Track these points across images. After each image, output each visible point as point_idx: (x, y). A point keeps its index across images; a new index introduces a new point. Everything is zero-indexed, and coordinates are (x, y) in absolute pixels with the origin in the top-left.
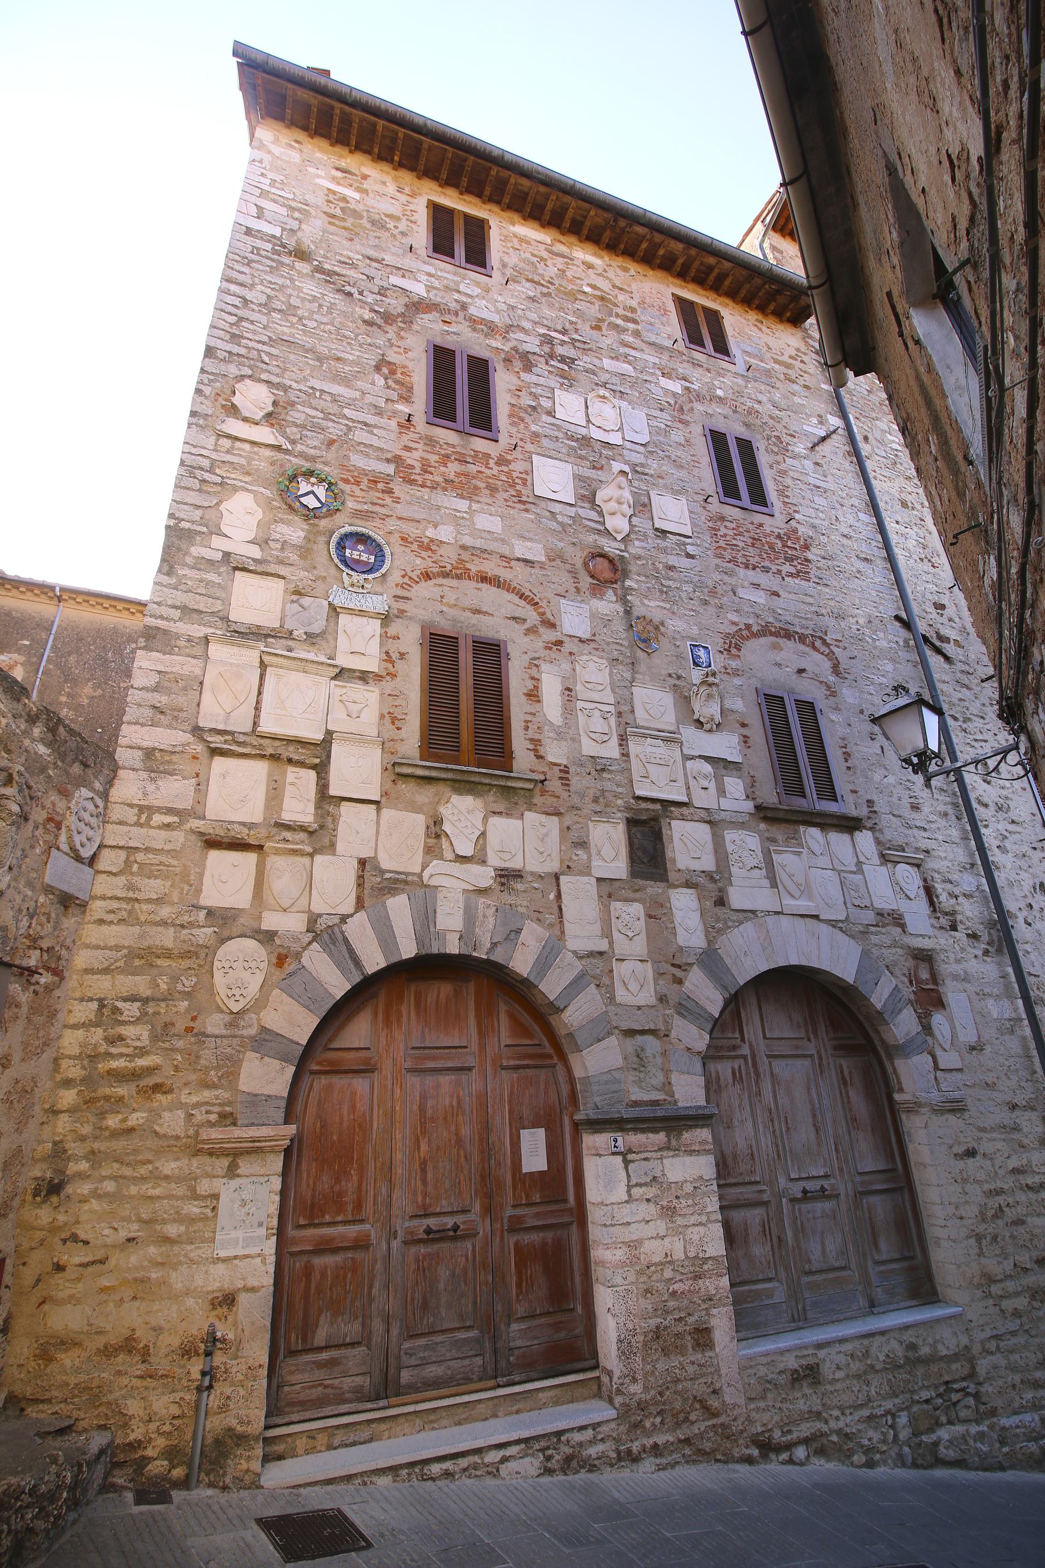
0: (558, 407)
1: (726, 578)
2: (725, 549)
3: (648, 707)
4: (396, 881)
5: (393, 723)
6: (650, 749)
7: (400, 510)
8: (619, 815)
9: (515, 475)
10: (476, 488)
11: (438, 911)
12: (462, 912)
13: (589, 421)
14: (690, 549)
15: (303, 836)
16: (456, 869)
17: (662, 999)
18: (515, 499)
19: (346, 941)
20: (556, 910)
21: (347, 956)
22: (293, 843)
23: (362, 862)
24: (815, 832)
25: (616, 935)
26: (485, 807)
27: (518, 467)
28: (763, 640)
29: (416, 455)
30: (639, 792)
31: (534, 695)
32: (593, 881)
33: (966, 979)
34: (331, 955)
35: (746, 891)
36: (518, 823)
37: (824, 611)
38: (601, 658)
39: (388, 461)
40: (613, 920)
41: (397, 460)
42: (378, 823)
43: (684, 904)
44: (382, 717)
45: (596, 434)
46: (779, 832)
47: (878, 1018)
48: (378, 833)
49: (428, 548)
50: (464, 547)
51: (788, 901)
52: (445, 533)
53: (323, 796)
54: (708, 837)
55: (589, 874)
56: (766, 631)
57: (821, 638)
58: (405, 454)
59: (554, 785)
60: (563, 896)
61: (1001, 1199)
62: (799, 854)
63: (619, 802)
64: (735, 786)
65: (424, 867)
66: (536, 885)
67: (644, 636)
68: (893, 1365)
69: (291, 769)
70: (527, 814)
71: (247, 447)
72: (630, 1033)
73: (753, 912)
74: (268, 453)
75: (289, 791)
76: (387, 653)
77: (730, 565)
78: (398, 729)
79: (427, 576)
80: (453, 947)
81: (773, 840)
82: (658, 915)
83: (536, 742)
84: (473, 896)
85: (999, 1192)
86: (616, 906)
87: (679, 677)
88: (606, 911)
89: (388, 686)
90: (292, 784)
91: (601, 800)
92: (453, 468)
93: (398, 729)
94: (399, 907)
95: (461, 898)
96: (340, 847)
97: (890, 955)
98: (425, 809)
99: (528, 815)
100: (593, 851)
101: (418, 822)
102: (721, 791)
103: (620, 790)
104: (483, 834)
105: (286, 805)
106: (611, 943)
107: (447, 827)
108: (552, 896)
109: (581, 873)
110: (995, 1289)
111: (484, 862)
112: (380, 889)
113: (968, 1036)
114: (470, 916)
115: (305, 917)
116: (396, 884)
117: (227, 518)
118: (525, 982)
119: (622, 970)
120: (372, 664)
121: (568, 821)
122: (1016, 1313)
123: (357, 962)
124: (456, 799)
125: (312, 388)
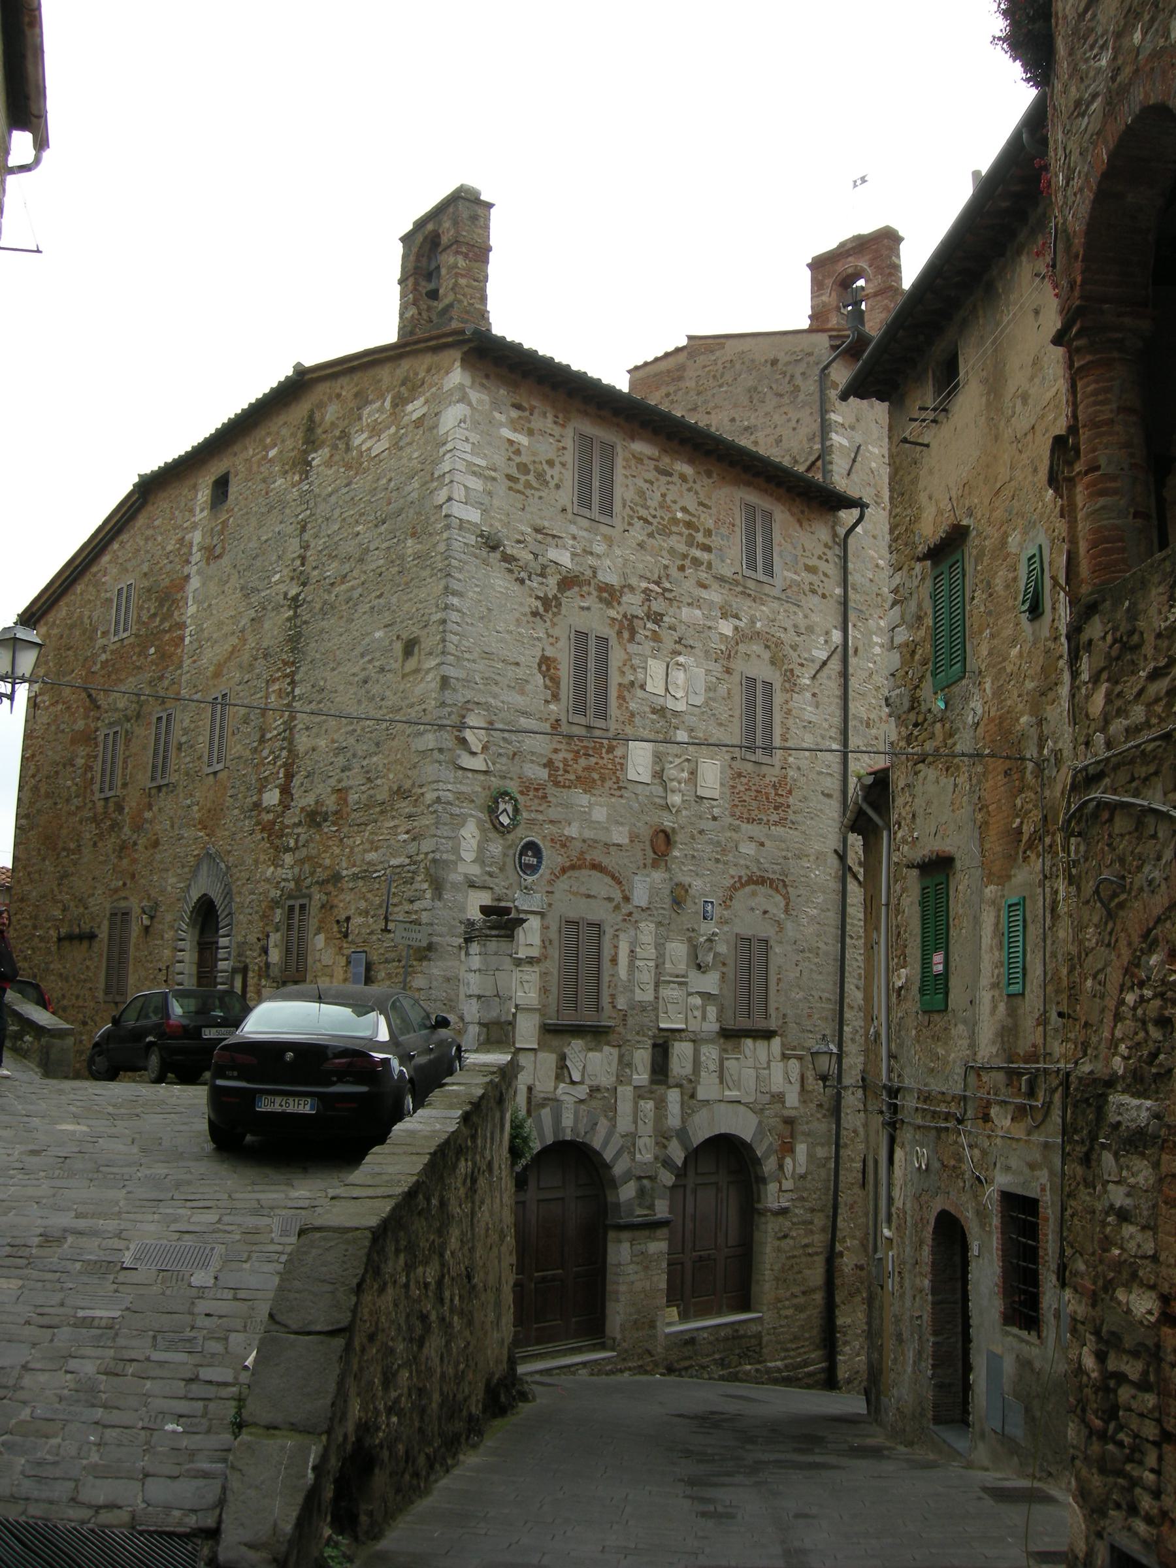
0: (649, 680)
1: (733, 834)
2: (737, 806)
4: (545, 1099)
7: (553, 813)
9: (617, 760)
10: (594, 781)
13: (667, 690)
14: (716, 811)
17: (656, 1158)
18: (615, 786)
24: (749, 1042)
25: (640, 1122)
27: (618, 752)
28: (748, 889)
29: (561, 756)
30: (662, 1026)
31: (614, 961)
32: (630, 1088)
33: (808, 1134)
35: (707, 1089)
37: (790, 855)
38: (652, 922)
39: (545, 766)
41: (549, 764)
43: (674, 1096)
45: (671, 704)
46: (729, 1045)
47: (757, 1162)
49: (564, 846)
50: (584, 841)
51: (727, 1093)
52: (572, 831)
54: (691, 1052)
56: (751, 881)
57: (783, 881)
58: (554, 757)
61: (793, 1261)
62: (737, 1059)
64: (712, 1011)
67: (679, 897)
68: (726, 1339)
71: (470, 775)
72: (639, 1178)
73: (708, 1101)
74: (482, 778)
76: (543, 941)
77: (738, 822)
79: (564, 870)
81: (725, 1051)
82: (661, 1105)
83: (613, 996)
85: (794, 1257)
86: (642, 1103)
87: (693, 930)
88: (636, 1104)
92: (583, 762)
94: (546, 1113)
97: (773, 1121)
99: (606, 1048)
102: (704, 1018)
107: (568, 1063)
110: (779, 1305)
113: (801, 1170)
117: (463, 843)
119: (640, 1143)
120: (535, 952)
122: (786, 1317)
125: (503, 702)
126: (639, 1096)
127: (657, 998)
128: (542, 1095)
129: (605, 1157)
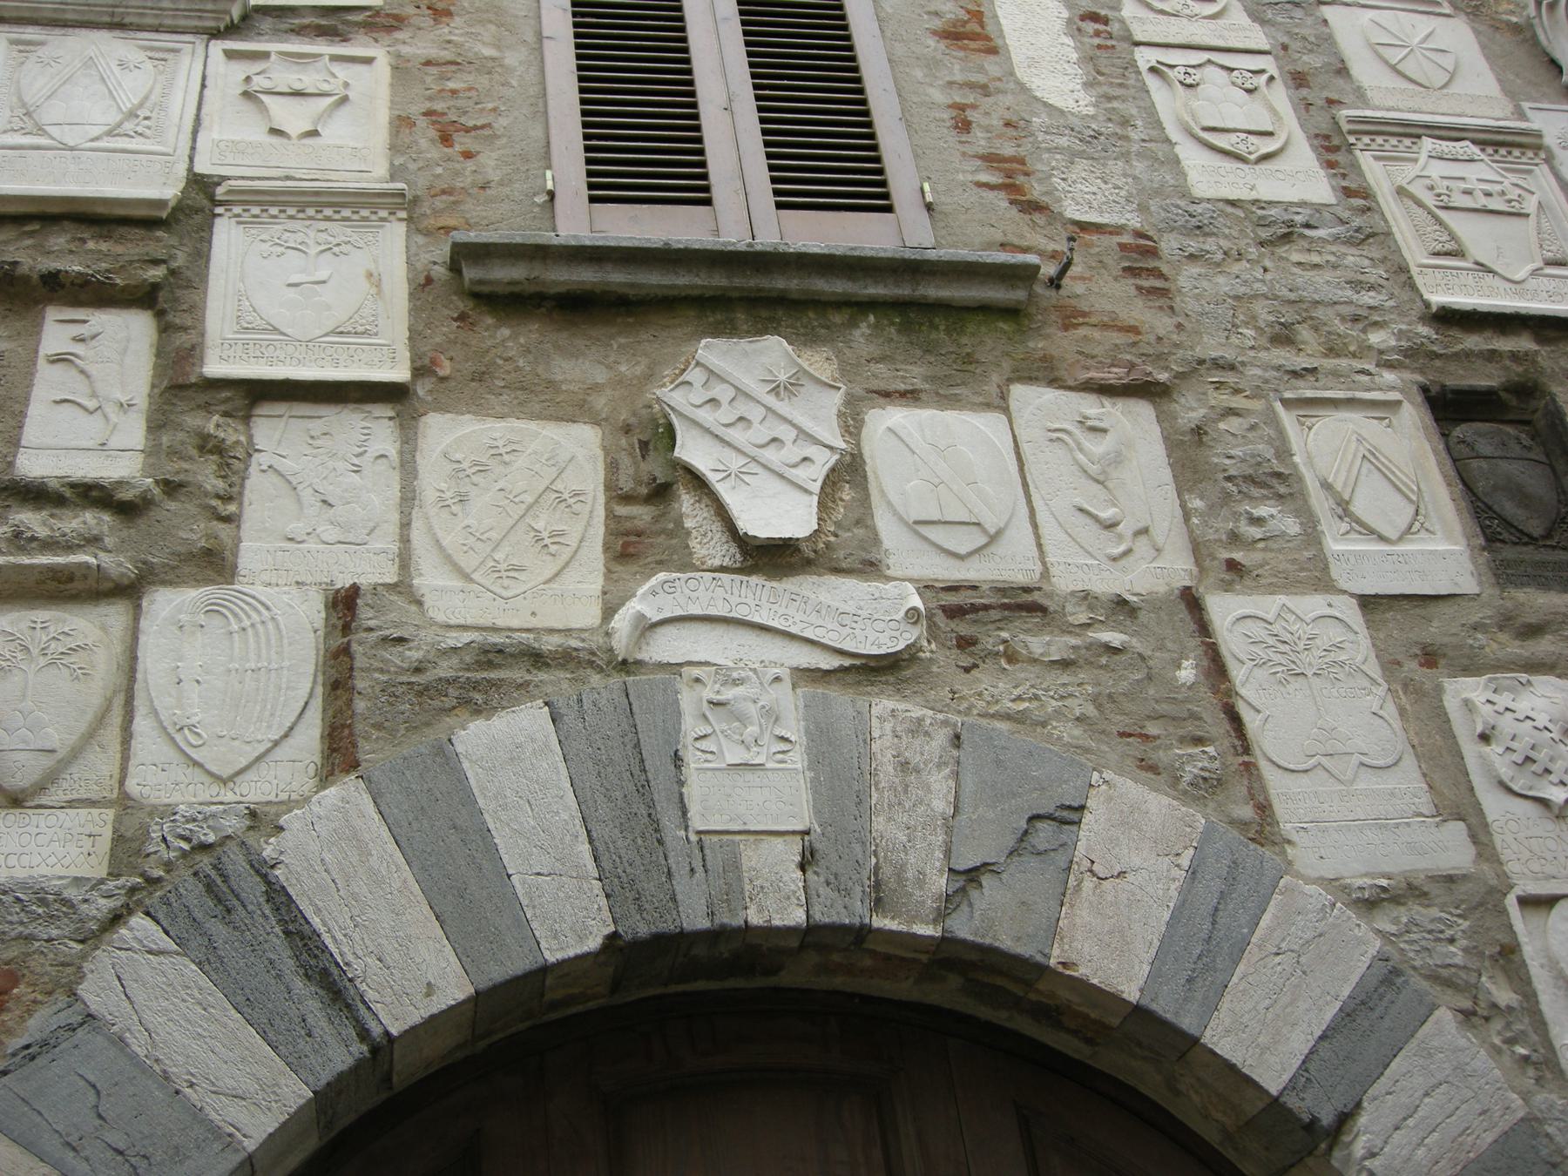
3: (1394, 56)
4: (491, 656)
5: (446, 139)
6: (1437, 170)
8: (1389, 377)
11: (693, 760)
12: (797, 759)
15: (90, 520)
16: (758, 597)
19: (278, 898)
20: (1216, 725)
21: (288, 964)
22: (48, 545)
23: (344, 604)
25: (1494, 805)
26: (847, 371)
32: (1349, 611)
34: (210, 962)
36: (988, 425)
40: (1471, 750)
42: (408, 467)
44: (401, 123)
48: (409, 498)
53: (182, 387)
55: (1322, 582)
59: (1101, 289)
60: (1237, 673)
63: (1375, 338)
65: (609, 612)
66: (1114, 638)
69: (53, 314)
70: (1018, 391)
75: (48, 383)
78: (468, 155)
80: (777, 899)
84: (841, 699)
86: (1465, 693)
89: (420, 44)
90: (59, 359)
91: (1304, 333)
93: (468, 155)
94: (513, 757)
95: (788, 700)
96: (252, 553)
98: (600, 402)
99: (1031, 399)
100: (1320, 503)
101: (574, 455)
103: (1368, 298)
104: (848, 472)
105: (30, 434)
106: (1480, 835)
107: (693, 451)
108: (1187, 673)
109: (1288, 583)
111: (870, 568)
112: (423, 691)
114: (840, 774)
115: (102, 822)
116: (498, 668)
118: (1142, 1026)
121: (1190, 409)
123: (334, 988)
124: (714, 351)
126: (1430, 657)
127: (1348, 193)
128: (467, 637)
129: (1222, 1039)
